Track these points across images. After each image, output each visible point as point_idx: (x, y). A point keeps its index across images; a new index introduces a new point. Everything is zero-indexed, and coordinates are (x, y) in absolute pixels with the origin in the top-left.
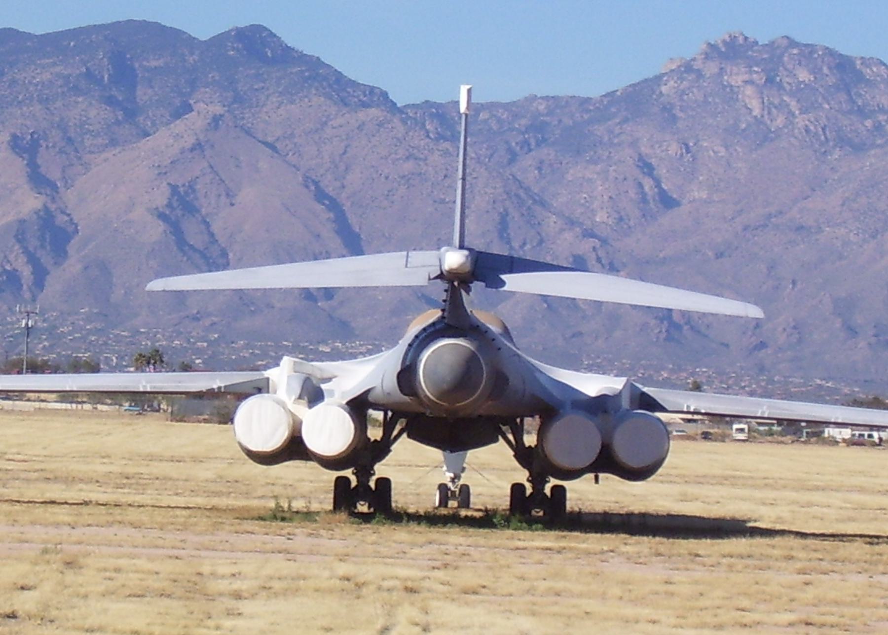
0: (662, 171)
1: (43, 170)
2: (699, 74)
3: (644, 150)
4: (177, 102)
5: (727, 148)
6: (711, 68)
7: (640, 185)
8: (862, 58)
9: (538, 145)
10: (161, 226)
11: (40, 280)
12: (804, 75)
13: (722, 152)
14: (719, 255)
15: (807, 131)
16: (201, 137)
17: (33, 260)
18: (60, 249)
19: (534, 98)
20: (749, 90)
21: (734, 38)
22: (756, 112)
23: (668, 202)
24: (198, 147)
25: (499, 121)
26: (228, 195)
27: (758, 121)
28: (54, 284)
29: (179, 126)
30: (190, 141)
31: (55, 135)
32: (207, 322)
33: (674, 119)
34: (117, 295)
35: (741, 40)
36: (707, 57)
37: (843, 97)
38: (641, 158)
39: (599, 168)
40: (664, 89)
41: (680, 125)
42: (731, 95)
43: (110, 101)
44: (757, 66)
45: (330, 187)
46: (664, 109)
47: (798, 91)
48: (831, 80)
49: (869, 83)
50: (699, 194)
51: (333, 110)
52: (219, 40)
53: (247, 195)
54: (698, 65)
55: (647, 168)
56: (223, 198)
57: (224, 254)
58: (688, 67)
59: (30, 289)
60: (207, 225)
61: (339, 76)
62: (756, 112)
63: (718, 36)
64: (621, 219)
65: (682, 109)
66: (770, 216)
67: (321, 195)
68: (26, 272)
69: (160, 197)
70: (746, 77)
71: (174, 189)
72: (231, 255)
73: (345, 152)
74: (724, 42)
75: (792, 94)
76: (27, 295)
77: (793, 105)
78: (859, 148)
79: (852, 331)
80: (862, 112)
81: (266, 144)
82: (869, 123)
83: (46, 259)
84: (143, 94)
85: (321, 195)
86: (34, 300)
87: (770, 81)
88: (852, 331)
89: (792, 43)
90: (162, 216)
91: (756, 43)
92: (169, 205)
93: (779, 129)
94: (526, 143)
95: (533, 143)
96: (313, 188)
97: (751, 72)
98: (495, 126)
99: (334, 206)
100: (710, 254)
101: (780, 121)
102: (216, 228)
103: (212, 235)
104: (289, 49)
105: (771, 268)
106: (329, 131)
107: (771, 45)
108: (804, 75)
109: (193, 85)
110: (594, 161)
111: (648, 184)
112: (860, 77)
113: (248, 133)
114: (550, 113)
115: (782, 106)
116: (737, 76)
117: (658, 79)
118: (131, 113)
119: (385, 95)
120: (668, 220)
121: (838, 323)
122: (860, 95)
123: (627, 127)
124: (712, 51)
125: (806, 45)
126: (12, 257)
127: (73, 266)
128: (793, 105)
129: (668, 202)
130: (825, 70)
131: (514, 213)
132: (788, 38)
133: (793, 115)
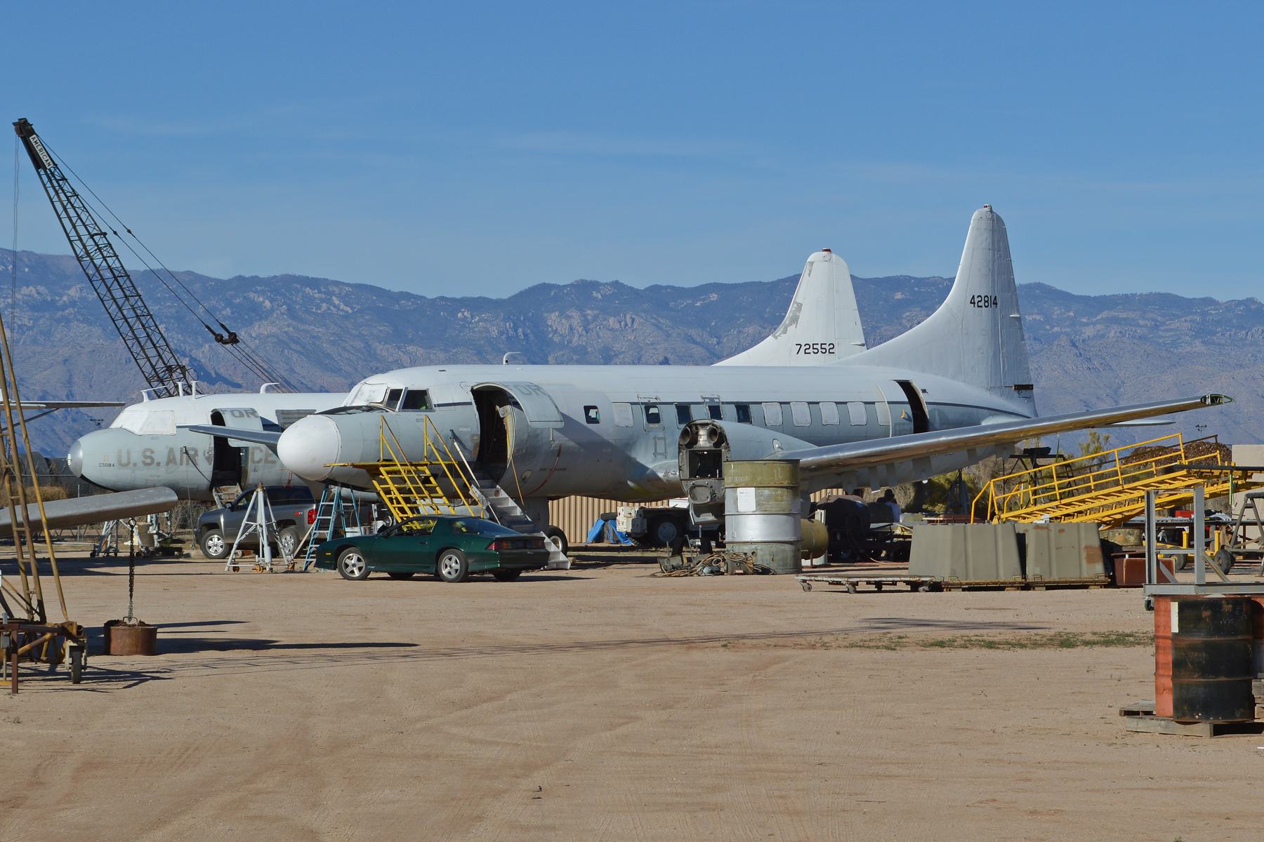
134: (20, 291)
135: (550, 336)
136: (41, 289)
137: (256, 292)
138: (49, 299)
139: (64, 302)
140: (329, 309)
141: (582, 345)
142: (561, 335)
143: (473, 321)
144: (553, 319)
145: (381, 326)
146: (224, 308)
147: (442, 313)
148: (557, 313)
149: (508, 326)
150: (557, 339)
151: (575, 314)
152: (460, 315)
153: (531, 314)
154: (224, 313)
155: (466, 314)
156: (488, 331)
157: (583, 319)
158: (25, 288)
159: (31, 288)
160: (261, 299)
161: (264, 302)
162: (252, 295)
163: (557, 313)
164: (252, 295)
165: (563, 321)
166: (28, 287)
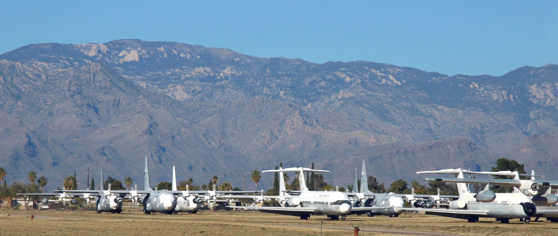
134: (194, 70)
135: (531, 99)
136: (208, 69)
137: (341, 71)
138: (212, 75)
139: (221, 77)
140: (387, 82)
141: (553, 106)
142: (538, 99)
143: (480, 90)
144: (533, 89)
145: (421, 93)
146: (321, 81)
147: (460, 85)
148: (536, 85)
149: (503, 93)
150: (535, 102)
151: (548, 86)
152: (471, 86)
153: (518, 86)
154: (320, 84)
155: (476, 85)
156: (490, 97)
157: (553, 88)
158: (197, 68)
159: (201, 68)
160: (344, 76)
161: (345, 78)
162: (338, 73)
163: (536, 85)
164: (338, 73)
165: (540, 90)
166: (199, 68)
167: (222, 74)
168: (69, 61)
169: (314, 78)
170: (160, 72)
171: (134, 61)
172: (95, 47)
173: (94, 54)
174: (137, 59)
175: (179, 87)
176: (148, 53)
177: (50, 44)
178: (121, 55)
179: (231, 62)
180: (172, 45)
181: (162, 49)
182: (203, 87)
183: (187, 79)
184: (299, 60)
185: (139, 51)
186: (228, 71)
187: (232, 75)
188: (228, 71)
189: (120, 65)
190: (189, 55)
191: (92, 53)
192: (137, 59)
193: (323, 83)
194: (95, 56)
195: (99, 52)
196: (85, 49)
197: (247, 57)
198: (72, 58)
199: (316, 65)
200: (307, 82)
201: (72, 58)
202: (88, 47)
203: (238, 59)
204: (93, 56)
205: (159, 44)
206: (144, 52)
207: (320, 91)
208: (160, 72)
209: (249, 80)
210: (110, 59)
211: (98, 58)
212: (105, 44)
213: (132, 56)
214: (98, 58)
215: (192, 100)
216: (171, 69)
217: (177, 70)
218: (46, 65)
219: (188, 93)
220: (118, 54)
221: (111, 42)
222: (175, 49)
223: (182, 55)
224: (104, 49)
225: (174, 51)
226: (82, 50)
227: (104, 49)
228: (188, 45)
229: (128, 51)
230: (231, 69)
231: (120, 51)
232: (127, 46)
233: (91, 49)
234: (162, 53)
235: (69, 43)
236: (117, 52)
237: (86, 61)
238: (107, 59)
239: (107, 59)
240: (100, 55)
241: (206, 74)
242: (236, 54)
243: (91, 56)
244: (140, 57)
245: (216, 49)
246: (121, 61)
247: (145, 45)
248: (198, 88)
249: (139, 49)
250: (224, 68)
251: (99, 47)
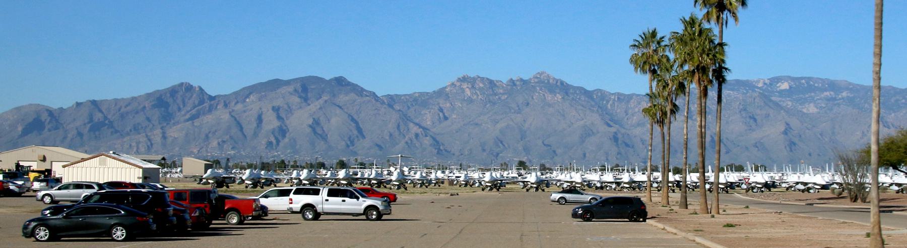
0: (445, 111)
1: (281, 115)
2: (455, 86)
3: (441, 105)
4: (318, 97)
5: (461, 104)
6: (458, 84)
7: (439, 115)
8: (496, 81)
9: (415, 104)
10: (310, 129)
11: (278, 142)
12: (481, 85)
13: (461, 105)
14: (457, 132)
15: (481, 99)
16: (322, 106)
17: (276, 139)
18: (284, 136)
19: (415, 93)
20: (467, 89)
21: (465, 76)
22: (469, 95)
23: (446, 118)
24: (321, 108)
25: (406, 99)
26: (328, 120)
27: (470, 97)
28: (281, 144)
29: (317, 103)
30: (319, 107)
31: (286, 106)
32: (320, 153)
33: (449, 97)
34: (298, 147)
35: (466, 77)
36: (458, 81)
37: (491, 90)
38: (440, 107)
39: (429, 110)
40: (447, 90)
41: (450, 99)
42: (463, 91)
43: (300, 97)
44: (470, 83)
45: (355, 117)
46: (446, 95)
47: (480, 89)
48: (488, 86)
49: (497, 86)
50: (454, 116)
51: (357, 98)
52: (331, 80)
53: (334, 121)
54: (455, 83)
55: (441, 110)
56: (327, 122)
57: (327, 135)
58: (453, 84)
59: (275, 146)
60: (322, 128)
61: (362, 88)
62: (469, 95)
63: (461, 76)
64: (433, 123)
65: (451, 94)
66: (470, 122)
67: (353, 120)
68: (274, 142)
69: (310, 121)
70: (467, 86)
71: (314, 119)
72: (328, 136)
73: (360, 108)
74: (462, 77)
75: (478, 90)
76: (274, 148)
77: (478, 92)
78: (494, 104)
79: (484, 150)
80: (496, 94)
81: (338, 106)
82: (497, 97)
83: (280, 138)
84: (309, 95)
85: (353, 120)
86: (276, 148)
87: (473, 87)
88: (484, 150)
89: (479, 77)
90: (310, 126)
91: (470, 77)
92: (312, 123)
93: (475, 99)
94: (412, 104)
95: (414, 104)
96: (350, 118)
97: (468, 85)
98: (405, 100)
99: (356, 123)
100: (454, 132)
101: (475, 97)
102: (324, 129)
103: (323, 130)
104: (349, 82)
105: (469, 135)
106: (356, 103)
107: (474, 78)
108: (481, 85)
109: (323, 92)
110: (428, 109)
111: (441, 114)
112: (495, 85)
113: (335, 104)
114: (419, 96)
115: (476, 93)
116: (465, 86)
117: (446, 88)
118: (306, 100)
119: (374, 93)
120: (448, 122)
121: (480, 148)
122: (495, 90)
123: (437, 100)
124: (459, 80)
125: (482, 78)
126: (270, 138)
127: (286, 140)
128: (478, 92)
129: (446, 118)
130: (487, 84)
131: (401, 123)
132: (478, 76)
133: (478, 95)
136: (832, 93)
138: (834, 96)
146: (902, 100)
166: (826, 91)
167: (840, 96)
168: (746, 90)
169: (898, 97)
170: (801, 96)
171: (786, 89)
172: (762, 81)
173: (761, 86)
174: (788, 88)
175: (812, 105)
176: (795, 84)
177: (735, 80)
178: (778, 85)
179: (847, 89)
180: (810, 79)
181: (803, 81)
182: (827, 104)
183: (818, 99)
184: (890, 86)
185: (789, 83)
186: (844, 94)
187: (847, 96)
188: (844, 94)
189: (777, 92)
190: (820, 85)
191: (760, 85)
192: (788, 88)
193: (903, 101)
194: (763, 87)
195: (765, 84)
196: (756, 83)
197: (858, 85)
198: (747, 88)
199: (901, 89)
200: (893, 100)
201: (747, 88)
202: (758, 81)
203: (851, 87)
204: (761, 87)
205: (802, 78)
206: (792, 83)
207: (901, 105)
208: (801, 96)
209: (857, 99)
210: (771, 88)
211: (764, 88)
212: (768, 79)
213: (785, 86)
214: (764, 88)
215: (819, 113)
216: (809, 94)
217: (813, 94)
218: (732, 92)
219: (817, 108)
220: (776, 86)
221: (772, 78)
222: (812, 81)
223: (816, 85)
224: (767, 82)
225: (811, 83)
226: (754, 83)
227: (767, 82)
228: (820, 79)
229: (782, 83)
230: (847, 93)
231: (777, 83)
232: (782, 80)
233: (759, 83)
234: (804, 84)
235: (746, 79)
236: (775, 84)
237: (756, 90)
238: (769, 88)
239: (769, 88)
240: (765, 86)
241: (830, 96)
242: (850, 84)
243: (759, 86)
244: (790, 87)
245: (837, 81)
246: (778, 89)
247: (793, 79)
248: (824, 106)
249: (790, 82)
250: (842, 92)
251: (764, 81)
